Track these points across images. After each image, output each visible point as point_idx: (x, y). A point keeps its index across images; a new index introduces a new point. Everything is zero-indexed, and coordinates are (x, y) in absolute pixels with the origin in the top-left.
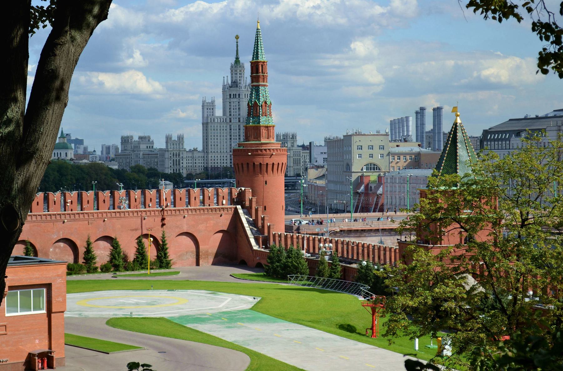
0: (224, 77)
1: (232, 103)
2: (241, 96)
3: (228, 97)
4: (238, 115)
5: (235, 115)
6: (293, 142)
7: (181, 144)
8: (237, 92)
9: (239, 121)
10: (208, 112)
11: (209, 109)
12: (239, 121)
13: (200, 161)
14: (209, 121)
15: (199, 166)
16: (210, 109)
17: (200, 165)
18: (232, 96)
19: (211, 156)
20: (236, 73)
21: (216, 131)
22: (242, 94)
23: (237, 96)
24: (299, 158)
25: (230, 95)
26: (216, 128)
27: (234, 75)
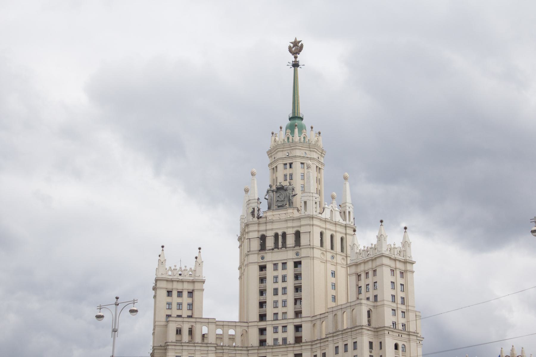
1: (270, 267)
2: (304, 240)
3: (255, 245)
4: (291, 314)
5: (280, 316)
8: (290, 224)
9: (298, 340)
10: (169, 304)
11: (175, 293)
12: (298, 340)
14: (172, 336)
16: (180, 294)
18: (270, 243)
20: (288, 161)
23: (290, 241)
25: (263, 238)
27: (281, 172)
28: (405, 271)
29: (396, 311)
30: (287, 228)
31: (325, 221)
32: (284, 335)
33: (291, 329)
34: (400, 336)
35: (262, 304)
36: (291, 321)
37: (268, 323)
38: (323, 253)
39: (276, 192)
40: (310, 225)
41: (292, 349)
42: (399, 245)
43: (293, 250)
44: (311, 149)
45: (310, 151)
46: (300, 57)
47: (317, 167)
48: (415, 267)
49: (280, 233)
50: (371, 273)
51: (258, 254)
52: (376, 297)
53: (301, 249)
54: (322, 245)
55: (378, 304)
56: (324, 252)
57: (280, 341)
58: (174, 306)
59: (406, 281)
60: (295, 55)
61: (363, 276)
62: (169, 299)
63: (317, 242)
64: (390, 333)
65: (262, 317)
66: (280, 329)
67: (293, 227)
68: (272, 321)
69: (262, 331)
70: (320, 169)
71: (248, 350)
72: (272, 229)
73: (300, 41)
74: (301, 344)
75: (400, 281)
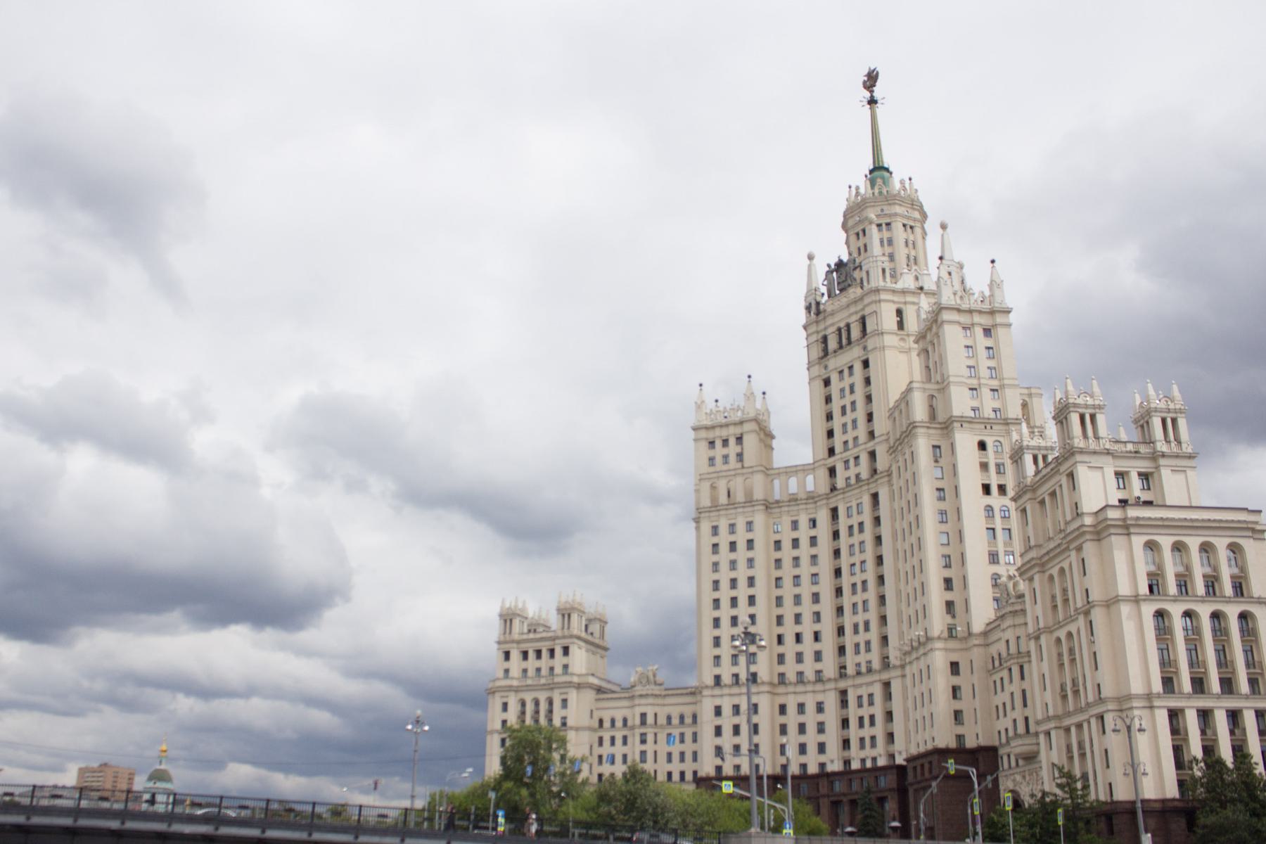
1: (834, 378)
3: (817, 352)
4: (863, 436)
6: (1145, 466)
7: (558, 651)
8: (853, 309)
10: (712, 460)
11: (718, 443)
13: (676, 749)
15: (670, 774)
16: (725, 443)
17: (676, 767)
18: (833, 345)
19: (718, 711)
20: (859, 229)
21: (742, 554)
22: (873, 307)
23: (856, 332)
24: (1232, 612)
26: (741, 537)
28: (993, 326)
29: (978, 390)
30: (852, 314)
31: (904, 292)
33: (864, 458)
34: (988, 427)
37: (837, 457)
38: (902, 339)
39: (837, 271)
40: (876, 302)
41: (866, 487)
43: (859, 345)
44: (890, 202)
45: (890, 204)
46: (878, 92)
47: (904, 225)
48: (1012, 318)
49: (842, 325)
51: (819, 363)
53: (866, 341)
54: (901, 325)
55: (945, 383)
56: (906, 338)
57: (853, 481)
58: (719, 460)
59: (997, 342)
60: (871, 89)
62: (711, 453)
63: (890, 321)
64: (964, 425)
65: (831, 452)
66: (852, 462)
67: (856, 313)
68: (841, 453)
69: (832, 471)
70: (911, 227)
71: (816, 502)
72: (832, 325)
73: (875, 69)
75: (982, 341)
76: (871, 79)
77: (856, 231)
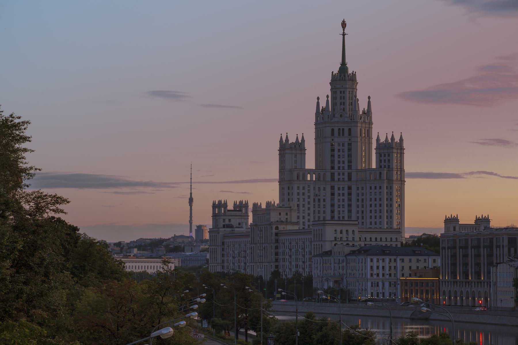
0: (318, 98)
4: (346, 168)
5: (341, 168)
9: (350, 179)
12: (350, 179)
14: (296, 178)
20: (342, 90)
25: (333, 130)
32: (343, 177)
33: (346, 174)
35: (333, 162)
36: (347, 171)
42: (398, 141)
49: (341, 128)
50: (387, 155)
52: (389, 166)
57: (341, 179)
61: (383, 155)
65: (333, 168)
66: (341, 174)
69: (333, 175)
74: (352, 182)
76: (344, 25)
77: (341, 90)
